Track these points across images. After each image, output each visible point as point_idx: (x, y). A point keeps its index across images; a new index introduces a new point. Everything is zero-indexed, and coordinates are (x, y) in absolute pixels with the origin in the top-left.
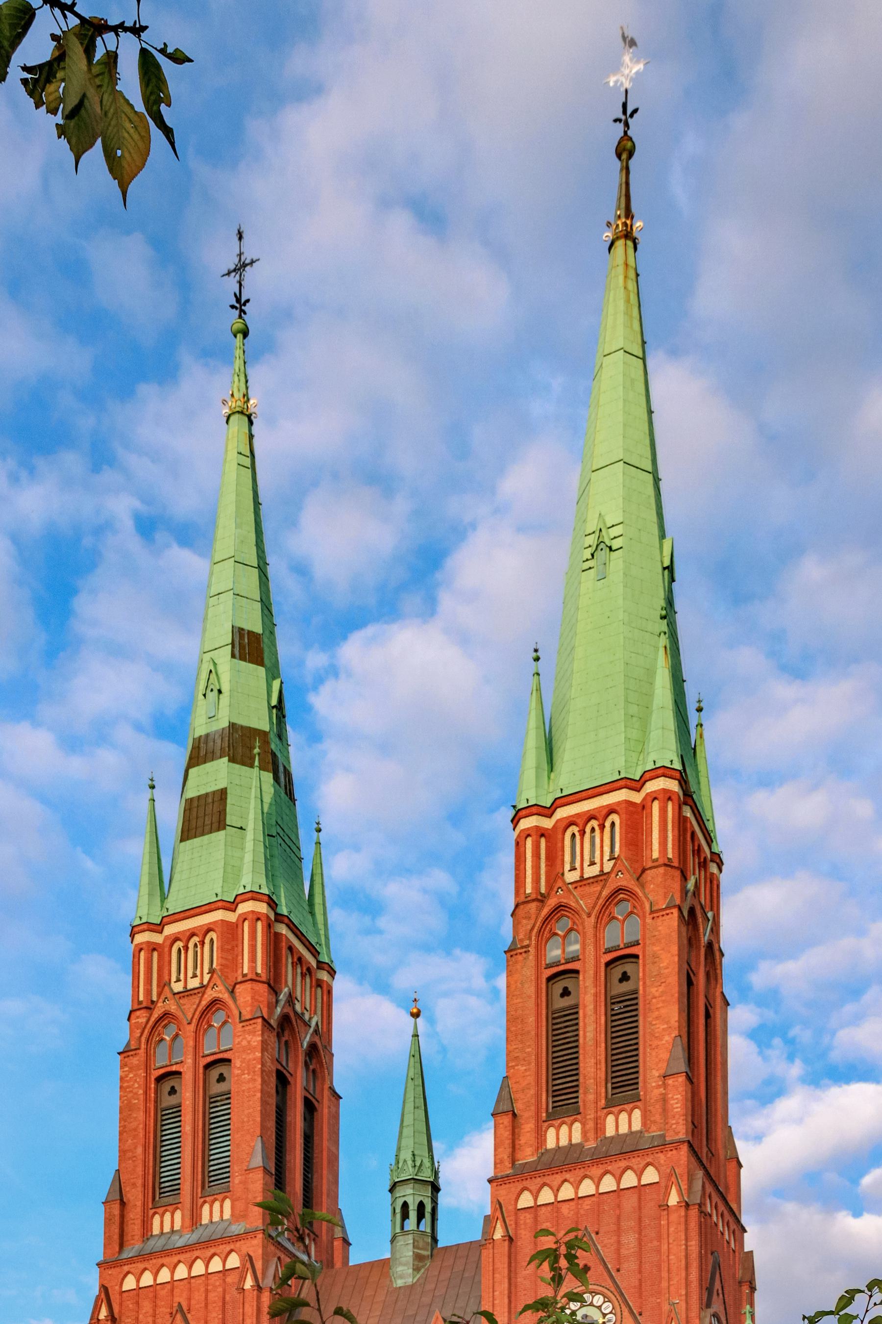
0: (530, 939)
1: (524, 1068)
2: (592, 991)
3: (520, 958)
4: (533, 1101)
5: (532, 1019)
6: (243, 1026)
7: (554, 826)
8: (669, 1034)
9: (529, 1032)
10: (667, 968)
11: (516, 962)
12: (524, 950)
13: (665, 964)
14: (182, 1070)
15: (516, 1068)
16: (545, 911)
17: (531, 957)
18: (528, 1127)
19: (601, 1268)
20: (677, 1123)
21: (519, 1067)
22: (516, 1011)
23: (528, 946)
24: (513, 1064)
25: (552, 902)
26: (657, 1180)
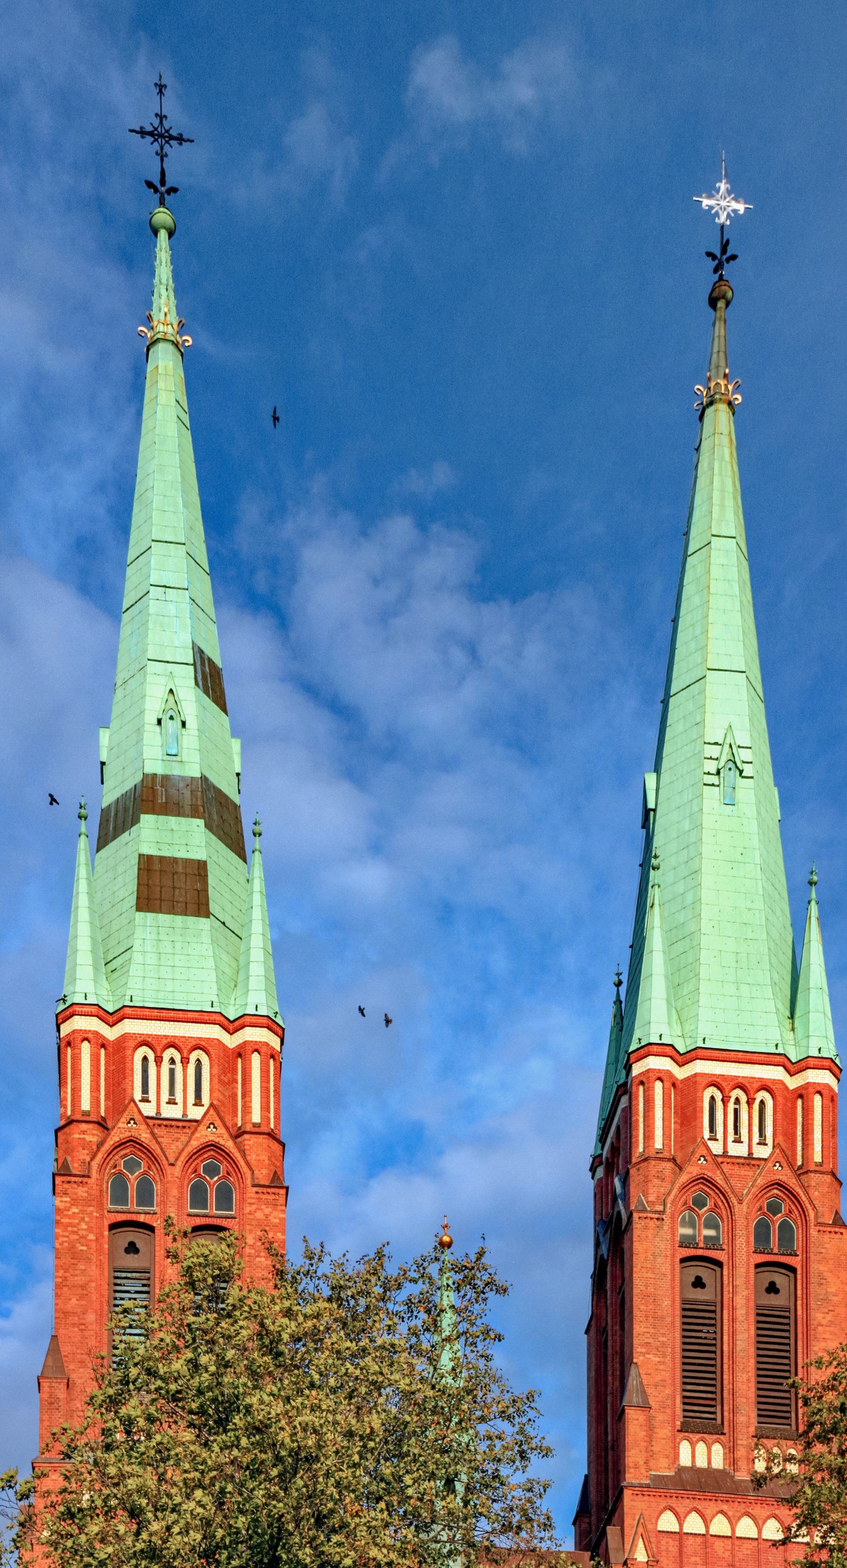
0: (665, 1205)
1: (657, 1359)
2: (744, 1293)
3: (652, 1224)
4: (669, 1402)
5: (667, 1303)
6: (257, 1193)
7: (687, 1079)
10: (835, 1295)
11: (646, 1228)
12: (657, 1216)
13: (833, 1290)
14: (155, 1225)
15: (647, 1356)
16: (684, 1178)
17: (666, 1228)
21: (651, 1356)
22: (646, 1286)
24: (643, 1350)
25: (692, 1171)
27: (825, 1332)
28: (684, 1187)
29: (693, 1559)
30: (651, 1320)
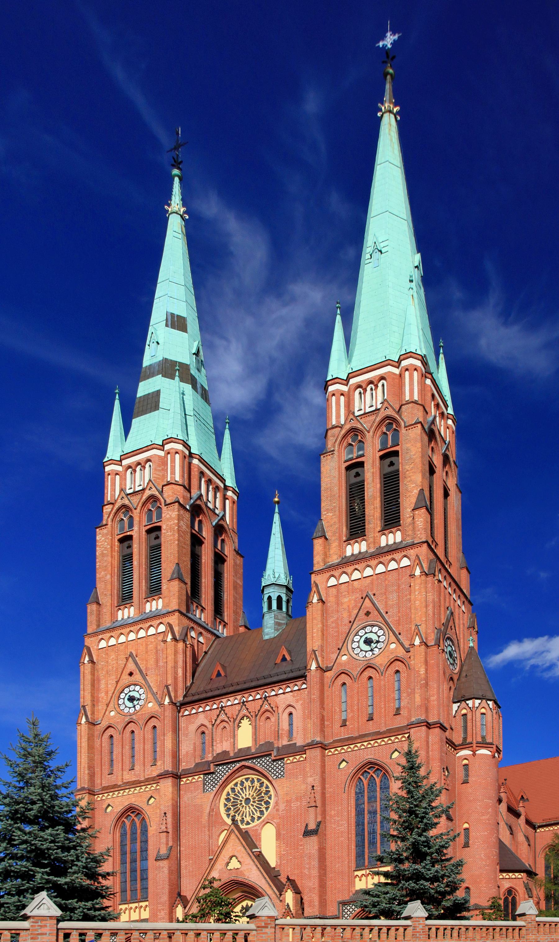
3: (329, 457)
4: (337, 531)
5: (336, 488)
8: (417, 489)
9: (334, 495)
10: (415, 455)
11: (327, 460)
16: (343, 432)
18: (334, 545)
19: (376, 613)
20: (421, 534)
23: (333, 451)
25: (348, 427)
26: (409, 564)
27: (409, 474)
28: (345, 436)
29: (344, 594)
30: (329, 498)
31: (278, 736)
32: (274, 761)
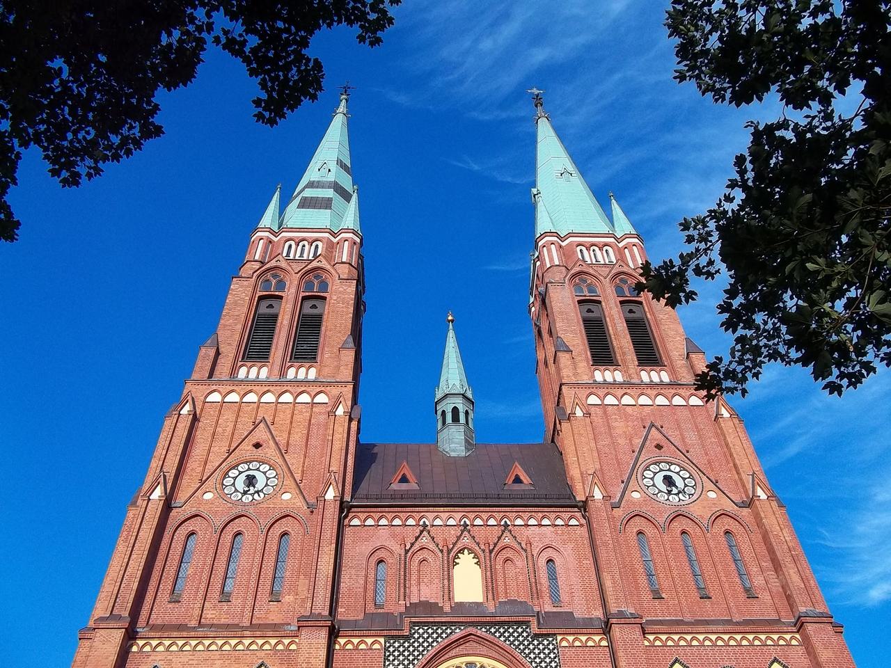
31: (536, 593)
32: (536, 636)
